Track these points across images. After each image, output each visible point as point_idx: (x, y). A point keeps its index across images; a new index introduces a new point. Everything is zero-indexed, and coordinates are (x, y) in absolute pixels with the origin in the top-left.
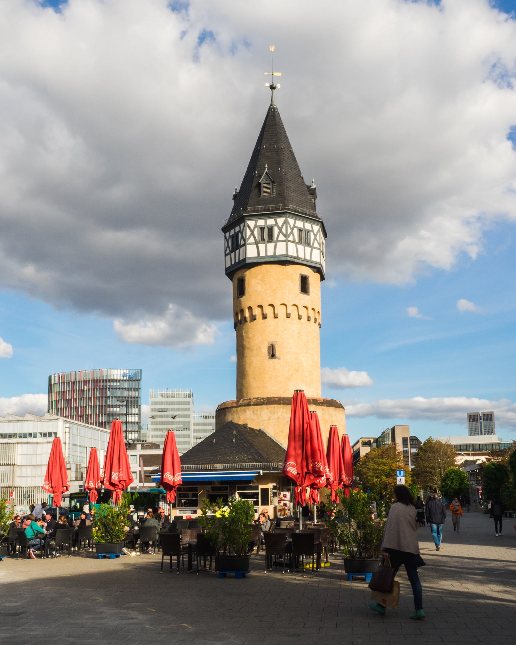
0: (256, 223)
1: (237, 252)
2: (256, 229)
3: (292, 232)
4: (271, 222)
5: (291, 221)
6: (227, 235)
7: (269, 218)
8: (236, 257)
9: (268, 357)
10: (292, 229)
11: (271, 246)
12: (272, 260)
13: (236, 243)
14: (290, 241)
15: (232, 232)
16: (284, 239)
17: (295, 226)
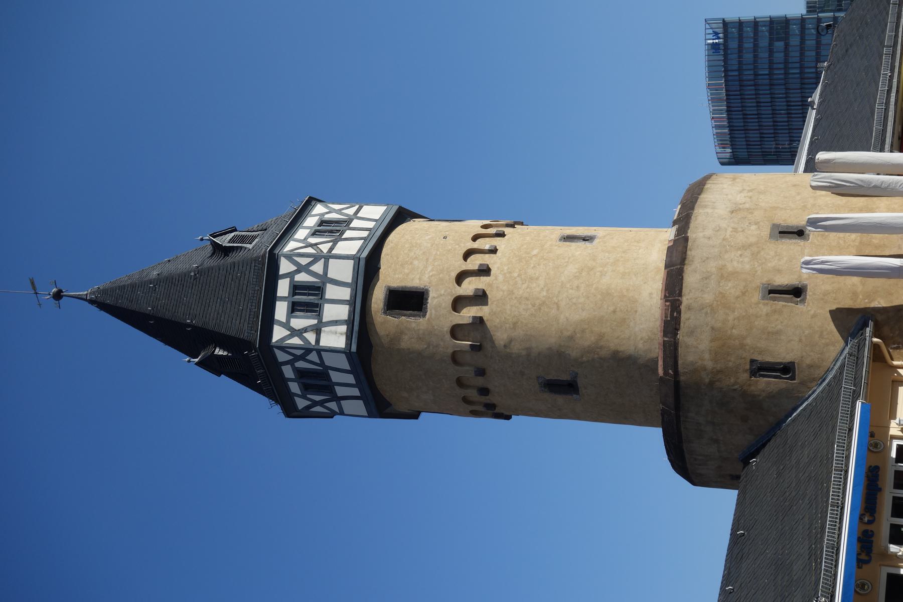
0: (281, 324)
4: (283, 289)
8: (344, 380)
11: (331, 292)
13: (317, 380)
15: (294, 387)
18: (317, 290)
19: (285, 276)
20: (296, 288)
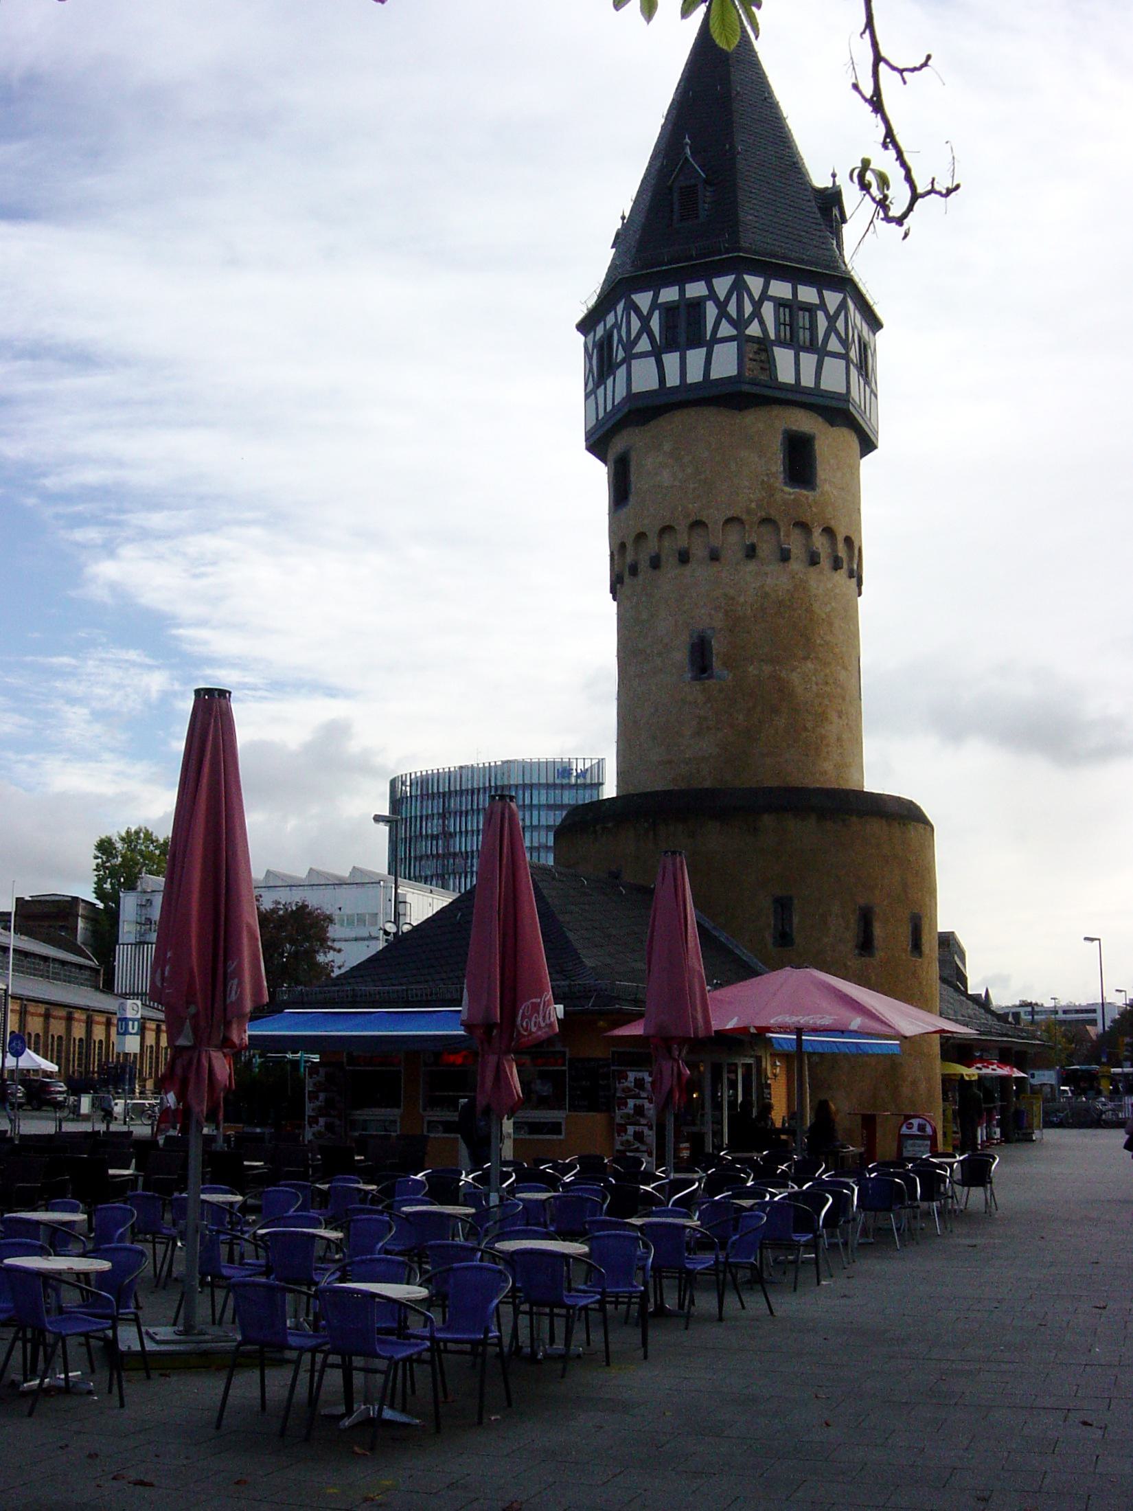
0: (656, 296)
1: (610, 382)
3: (757, 314)
4: (696, 289)
5: (755, 283)
10: (757, 305)
11: (696, 357)
16: (735, 332)
18: (696, 339)
19: (710, 287)
20: (697, 306)
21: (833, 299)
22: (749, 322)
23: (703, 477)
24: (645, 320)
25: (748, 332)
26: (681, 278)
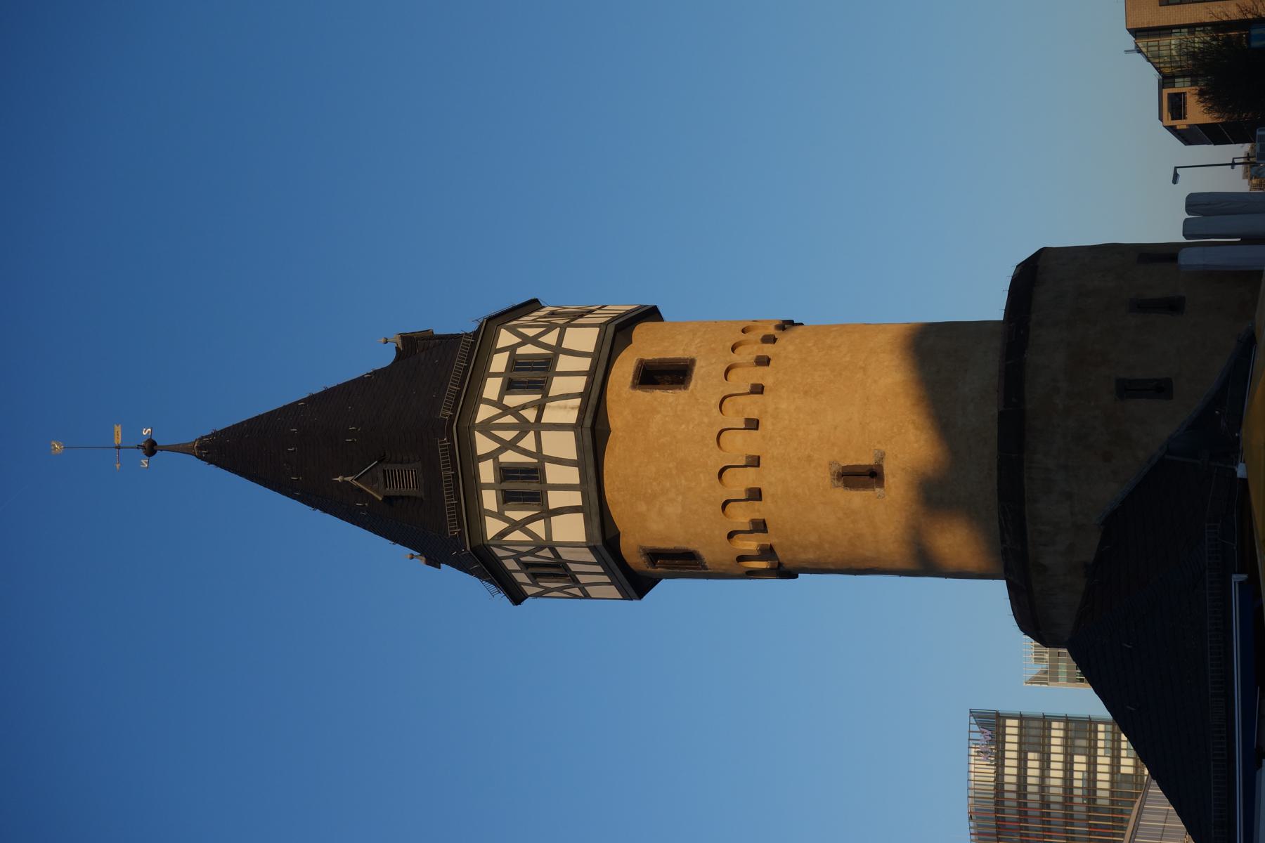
0: (492, 514)
1: (573, 567)
2: (507, 513)
3: (514, 411)
4: (487, 472)
5: (484, 413)
6: (530, 590)
7: (476, 475)
9: (878, 490)
10: (506, 410)
11: (554, 474)
12: (591, 471)
13: (552, 570)
14: (539, 417)
16: (532, 434)
17: (498, 403)
18: (534, 473)
20: (505, 473)
21: (506, 338)
22: (524, 420)
23: (674, 472)
24: (515, 525)
25: (532, 419)
26: (474, 488)
